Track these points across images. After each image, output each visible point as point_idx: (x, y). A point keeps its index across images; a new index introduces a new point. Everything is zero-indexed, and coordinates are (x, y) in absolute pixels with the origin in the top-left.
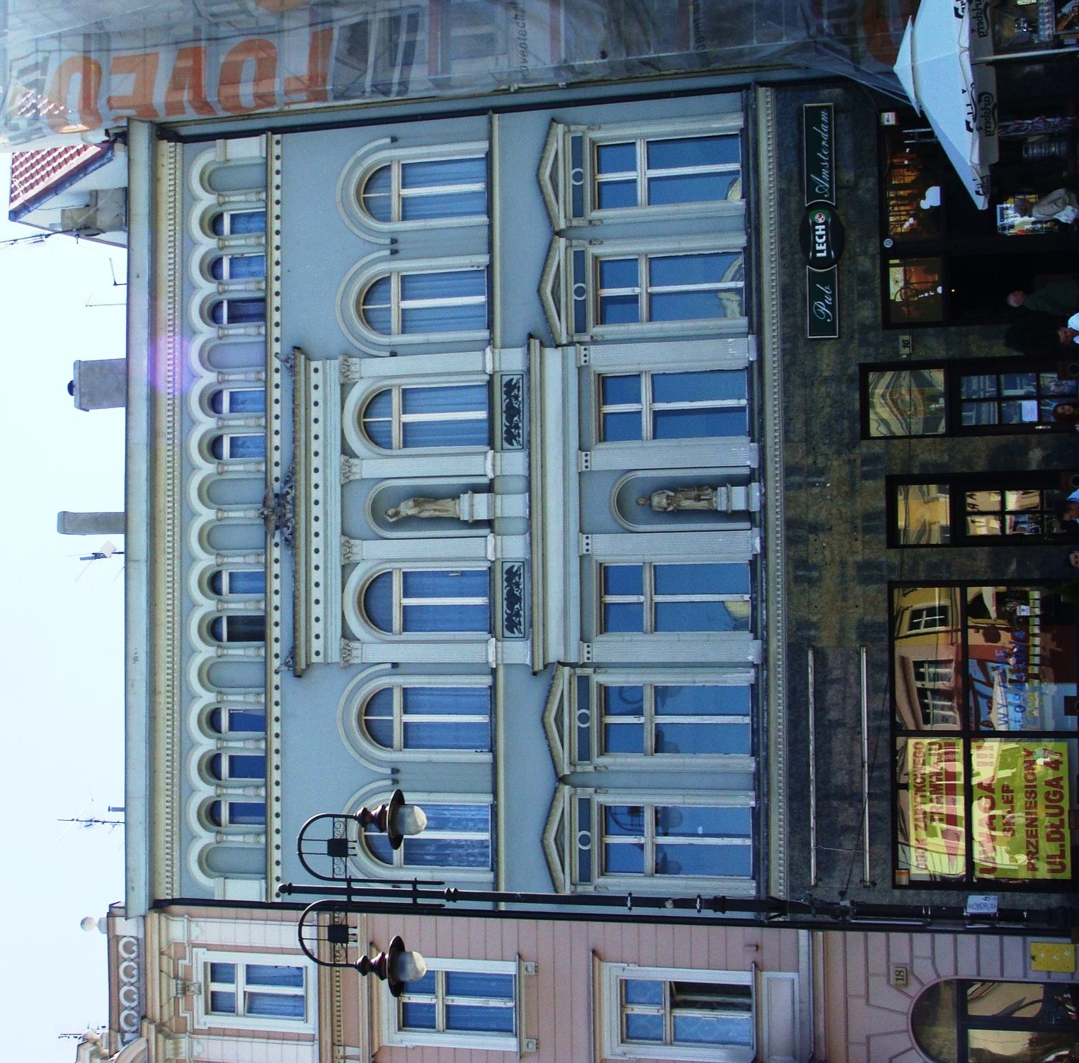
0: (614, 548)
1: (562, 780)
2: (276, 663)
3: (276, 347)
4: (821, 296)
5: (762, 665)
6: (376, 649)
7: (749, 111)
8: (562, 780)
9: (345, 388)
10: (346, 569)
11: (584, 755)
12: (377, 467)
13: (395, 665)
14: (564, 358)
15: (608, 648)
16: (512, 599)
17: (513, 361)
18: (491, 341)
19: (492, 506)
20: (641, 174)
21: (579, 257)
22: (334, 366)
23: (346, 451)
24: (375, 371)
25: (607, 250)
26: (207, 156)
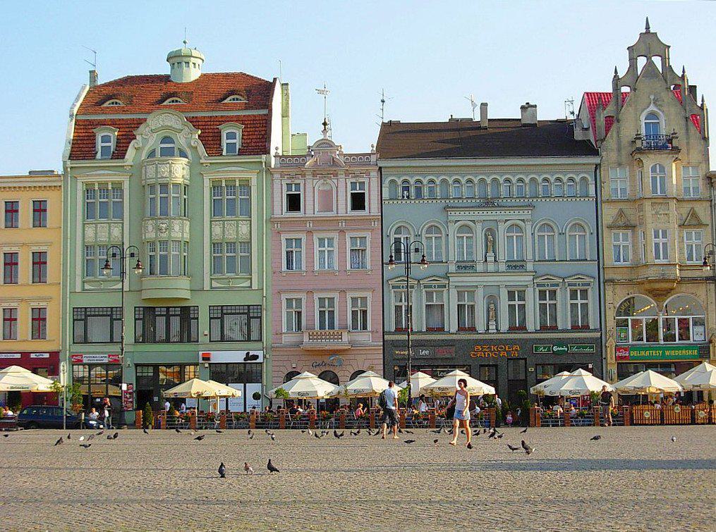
0: (480, 293)
1: (419, 281)
2: (447, 201)
3: (535, 200)
4: (544, 348)
5: (449, 333)
6: (453, 228)
7: (595, 330)
8: (419, 281)
9: (523, 220)
10: (473, 221)
11: (425, 287)
12: (502, 228)
13: (448, 235)
14: (529, 281)
15: (454, 292)
16: (465, 267)
17: (530, 267)
18: (535, 261)
19: (491, 262)
20: (579, 301)
21: (558, 285)
22: (529, 217)
23: (507, 220)
24: (528, 228)
25: (558, 293)
26: (591, 179)
